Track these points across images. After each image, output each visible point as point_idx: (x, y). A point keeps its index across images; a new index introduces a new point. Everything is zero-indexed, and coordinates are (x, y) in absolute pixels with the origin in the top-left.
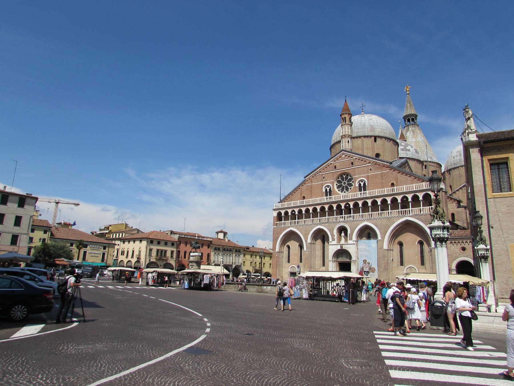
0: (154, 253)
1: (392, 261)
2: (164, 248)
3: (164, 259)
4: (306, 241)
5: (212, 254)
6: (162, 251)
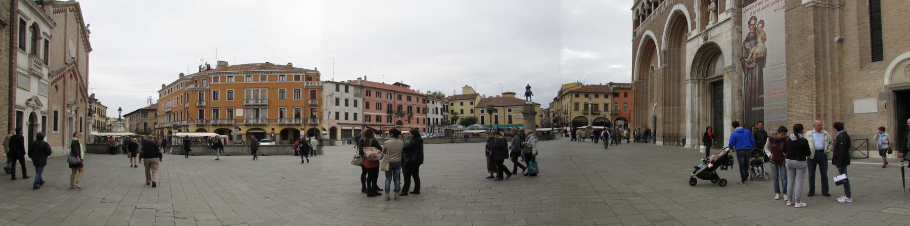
0: (581, 107)
1: (836, 46)
2: (595, 100)
4: (660, 48)
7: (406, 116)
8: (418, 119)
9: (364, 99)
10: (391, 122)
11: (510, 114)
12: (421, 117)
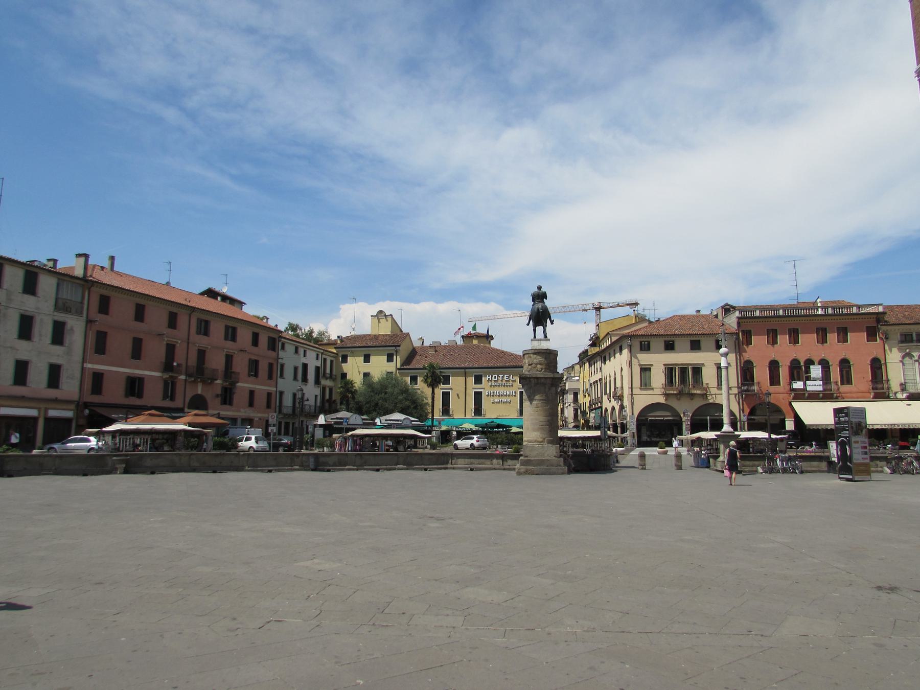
0: (658, 378)
3: (695, 394)
5: (893, 357)
6: (683, 370)
7: (219, 382)
8: (252, 393)
9: (89, 322)
10: (172, 398)
12: (261, 388)
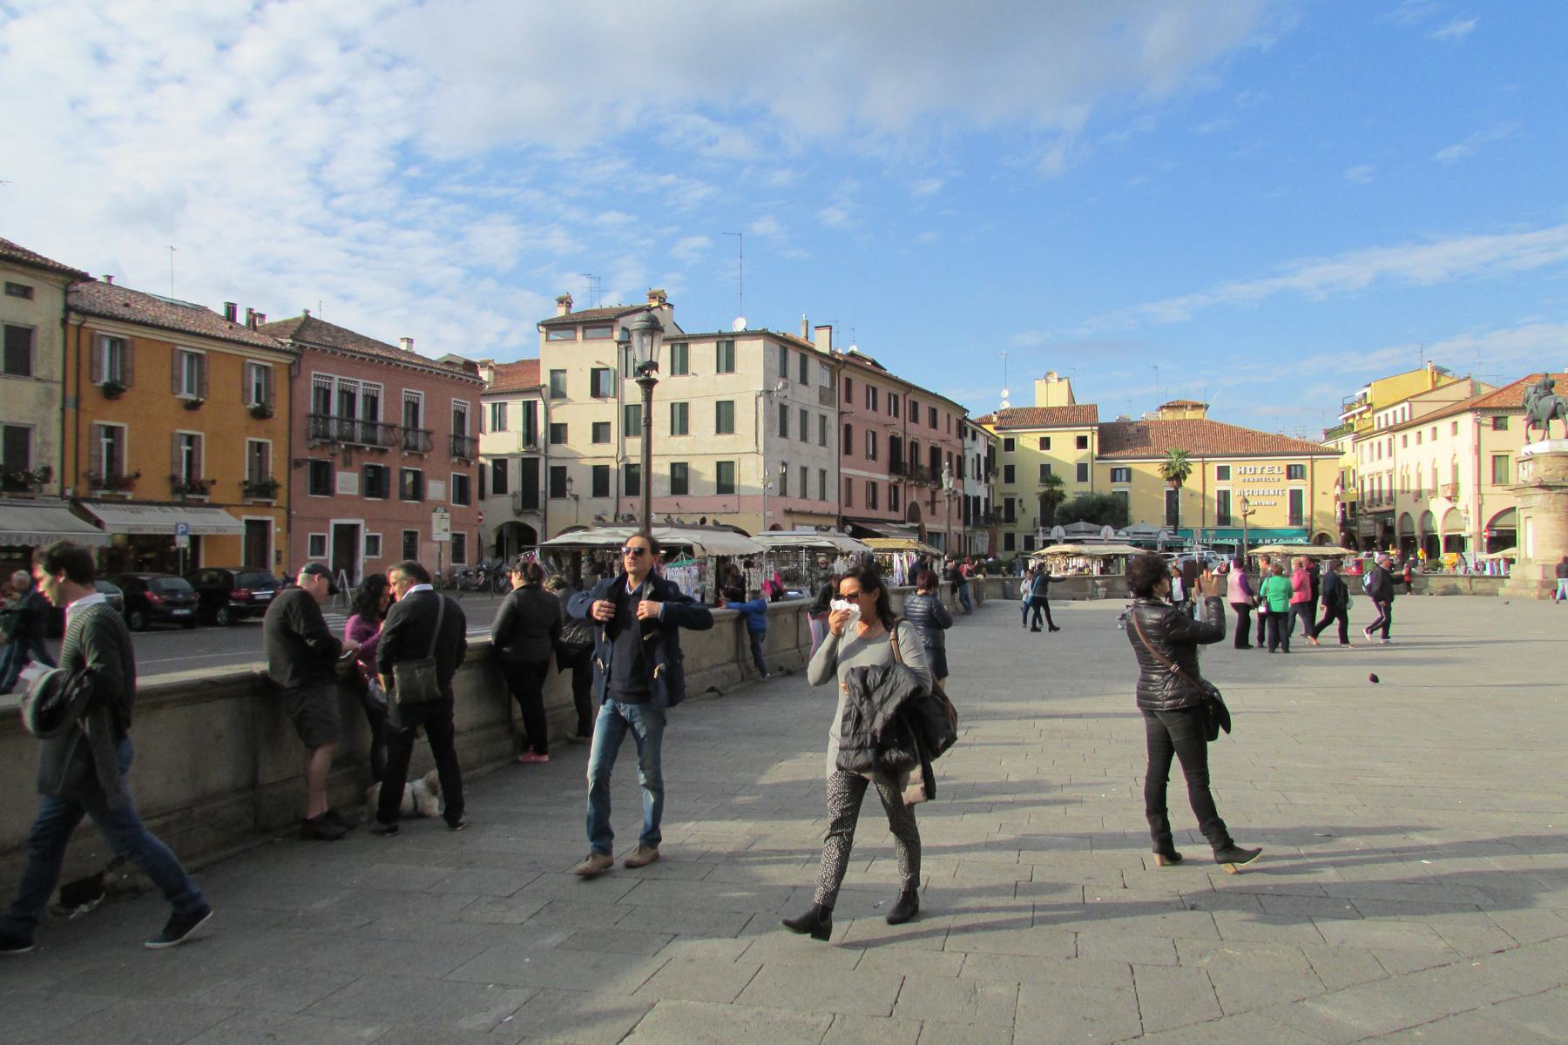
9: (841, 414)
11: (1223, 485)
